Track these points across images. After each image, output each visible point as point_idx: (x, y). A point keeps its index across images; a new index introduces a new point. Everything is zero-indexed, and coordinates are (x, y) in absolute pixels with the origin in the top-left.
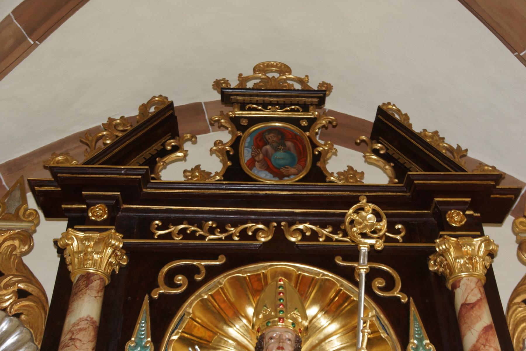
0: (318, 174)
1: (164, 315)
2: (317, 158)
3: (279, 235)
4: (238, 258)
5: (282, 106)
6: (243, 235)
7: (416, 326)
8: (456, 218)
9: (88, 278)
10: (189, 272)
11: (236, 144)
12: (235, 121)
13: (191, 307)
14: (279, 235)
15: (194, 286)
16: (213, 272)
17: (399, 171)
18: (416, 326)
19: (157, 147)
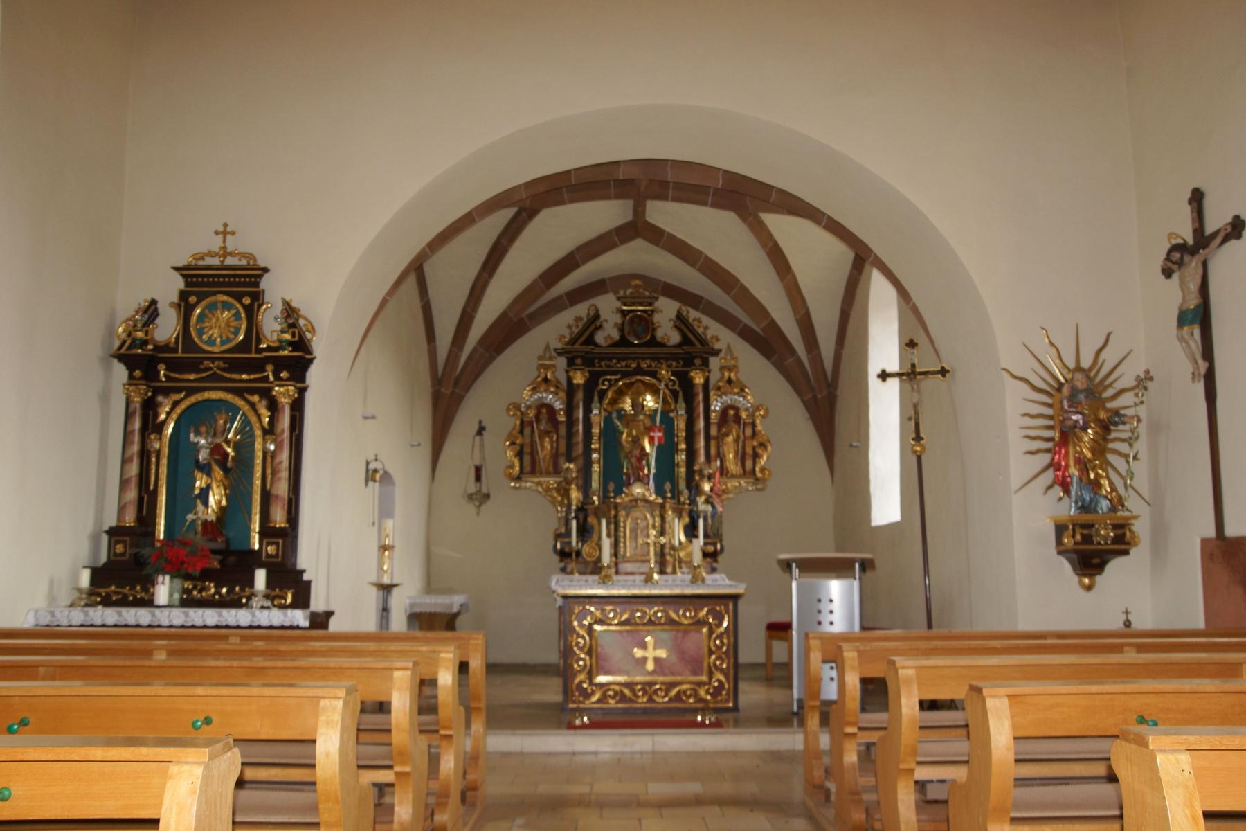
0: (653, 337)
1: (602, 394)
2: (654, 330)
3: (639, 365)
4: (625, 375)
5: (641, 304)
6: (627, 366)
7: (681, 399)
8: (698, 362)
9: (578, 385)
10: (609, 380)
11: (623, 324)
12: (622, 312)
13: (610, 394)
14: (639, 365)
15: (610, 386)
16: (617, 381)
17: (684, 336)
18: (681, 399)
19: (593, 327)
